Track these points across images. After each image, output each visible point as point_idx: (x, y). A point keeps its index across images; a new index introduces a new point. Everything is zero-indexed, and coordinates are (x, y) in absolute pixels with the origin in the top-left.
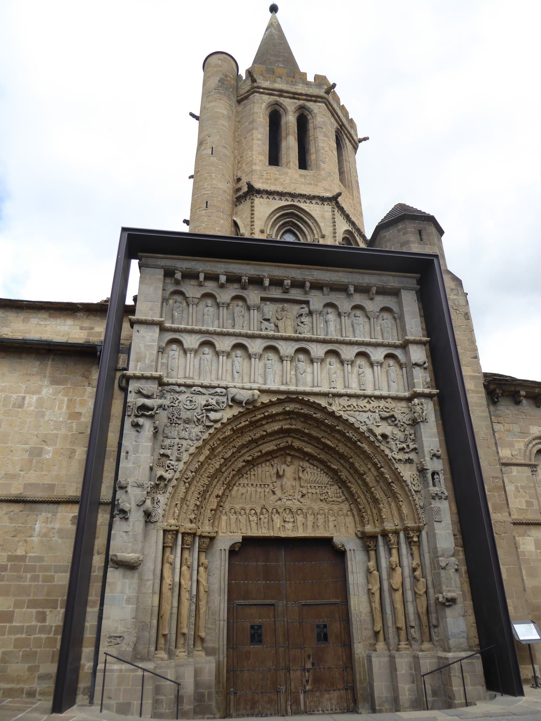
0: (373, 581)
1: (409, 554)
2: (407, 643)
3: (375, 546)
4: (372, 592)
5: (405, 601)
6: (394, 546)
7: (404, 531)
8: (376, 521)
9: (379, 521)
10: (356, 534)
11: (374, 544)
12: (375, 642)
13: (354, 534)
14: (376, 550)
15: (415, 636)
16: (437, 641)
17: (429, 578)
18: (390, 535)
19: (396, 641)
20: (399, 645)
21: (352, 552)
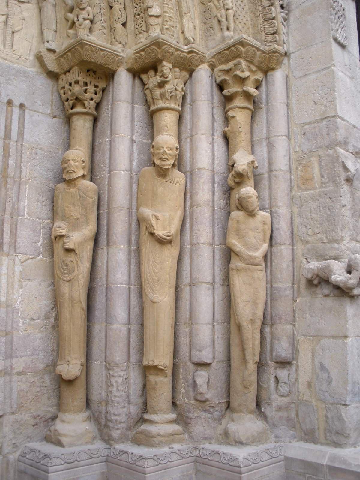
0: (75, 212)
1: (218, 134)
2: (173, 416)
3: (98, 106)
4: (70, 246)
5: (186, 279)
6: (173, 105)
7: (212, 67)
8: (119, 26)
9: (131, 25)
10: (39, 58)
11: (97, 98)
12: (53, 409)
13: (32, 58)
14: (95, 120)
15: (208, 396)
16: (279, 409)
17: (283, 211)
18: (167, 66)
19: (134, 409)
20: (142, 420)
21: (16, 111)
